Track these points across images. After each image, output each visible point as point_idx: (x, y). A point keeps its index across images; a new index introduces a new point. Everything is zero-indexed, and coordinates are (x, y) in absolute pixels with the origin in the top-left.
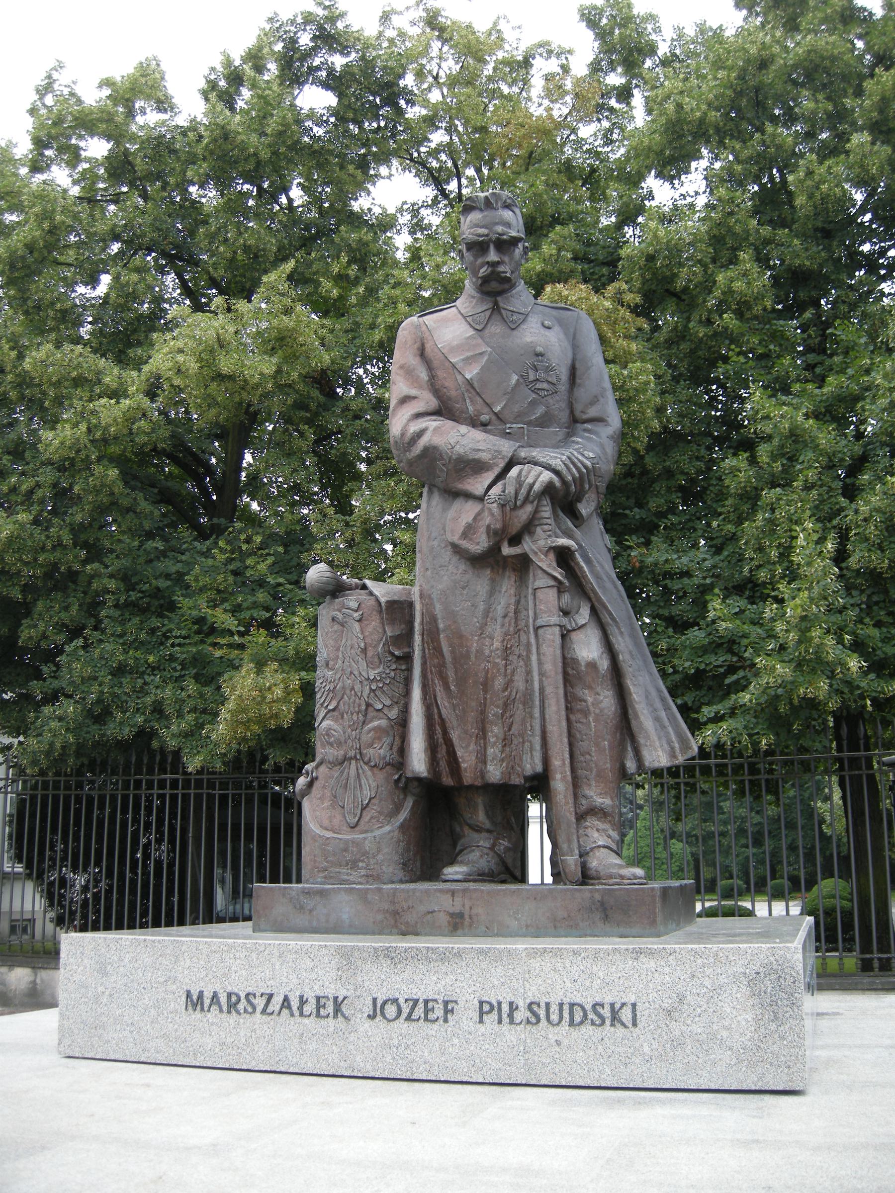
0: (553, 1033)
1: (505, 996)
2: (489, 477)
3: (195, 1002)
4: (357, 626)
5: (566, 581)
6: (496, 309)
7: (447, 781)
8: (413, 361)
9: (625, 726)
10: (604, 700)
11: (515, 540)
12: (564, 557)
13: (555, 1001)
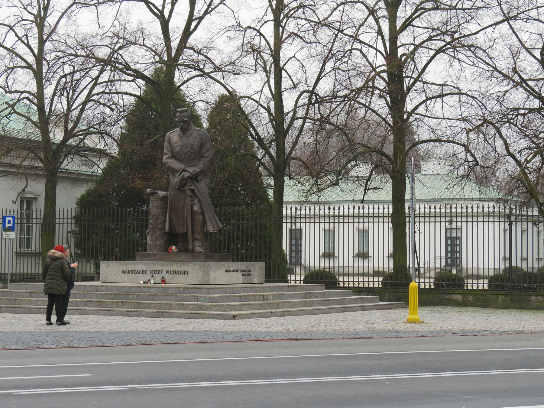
0: (177, 276)
1: (169, 270)
3: (123, 272)
6: (184, 133)
7: (174, 232)
8: (168, 145)
9: (204, 223)
10: (200, 218)
11: (183, 187)
12: (192, 191)
13: (177, 270)
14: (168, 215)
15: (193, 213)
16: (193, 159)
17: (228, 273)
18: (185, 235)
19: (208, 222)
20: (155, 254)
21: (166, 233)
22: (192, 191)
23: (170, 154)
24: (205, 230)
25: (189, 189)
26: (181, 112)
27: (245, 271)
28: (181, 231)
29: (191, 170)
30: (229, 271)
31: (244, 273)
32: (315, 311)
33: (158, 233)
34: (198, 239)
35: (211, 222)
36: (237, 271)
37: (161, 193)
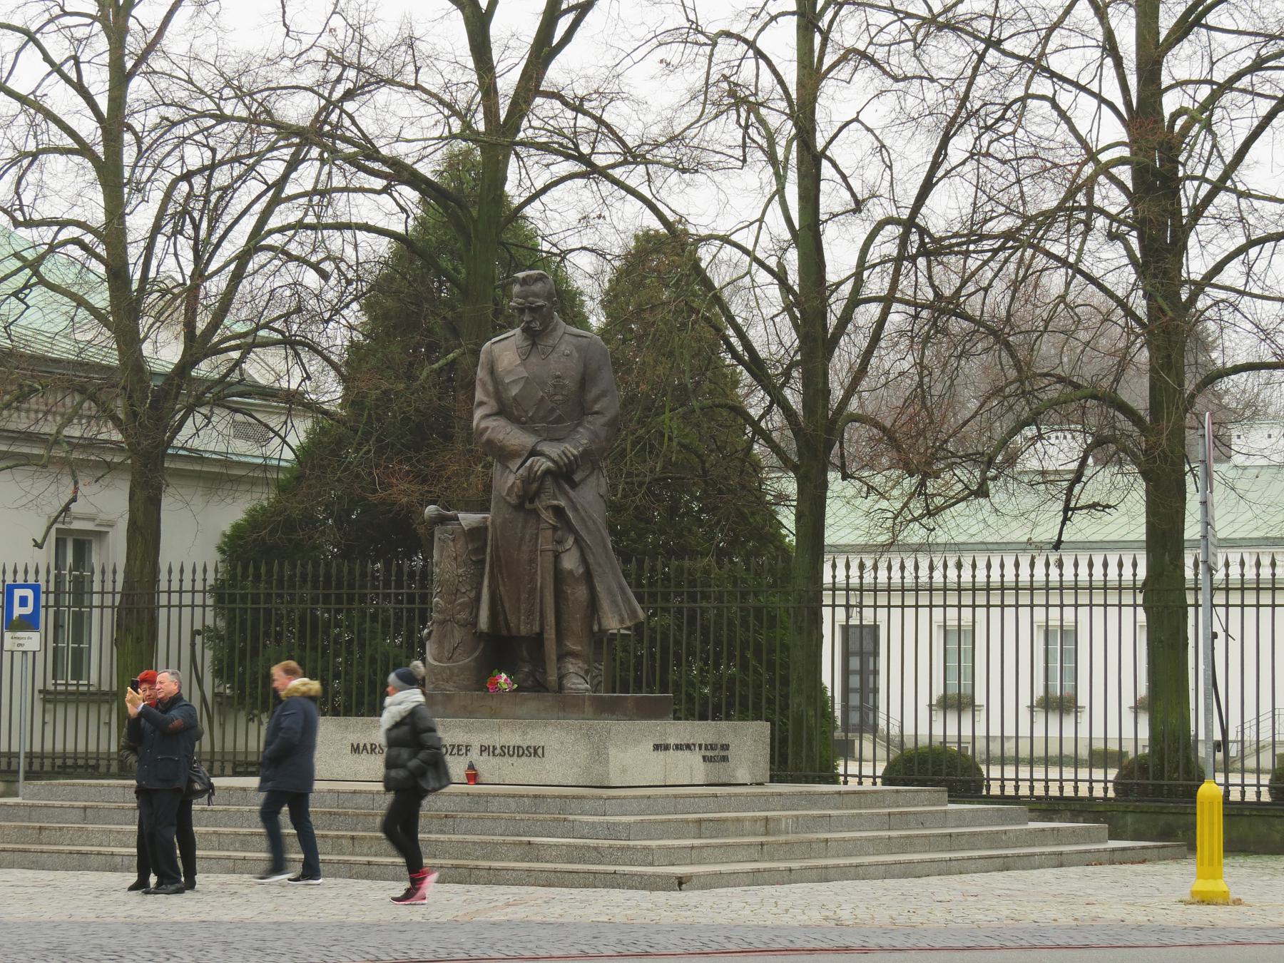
0: (511, 760)
2: (519, 461)
3: (356, 749)
4: (451, 544)
6: (534, 344)
7: (504, 632)
8: (487, 379)
9: (593, 606)
10: (581, 592)
11: (532, 501)
13: (512, 744)
14: (486, 582)
15: (559, 576)
16: (559, 420)
17: (661, 755)
18: (537, 641)
19: (605, 604)
20: (448, 698)
21: (480, 636)
22: (558, 511)
23: (492, 405)
24: (596, 628)
25: (547, 508)
26: (524, 282)
27: (712, 747)
28: (524, 630)
29: (553, 450)
30: (667, 747)
31: (709, 753)
32: (919, 867)
33: (456, 634)
34: (575, 655)
35: (614, 602)
36: (688, 747)
37: (468, 519)
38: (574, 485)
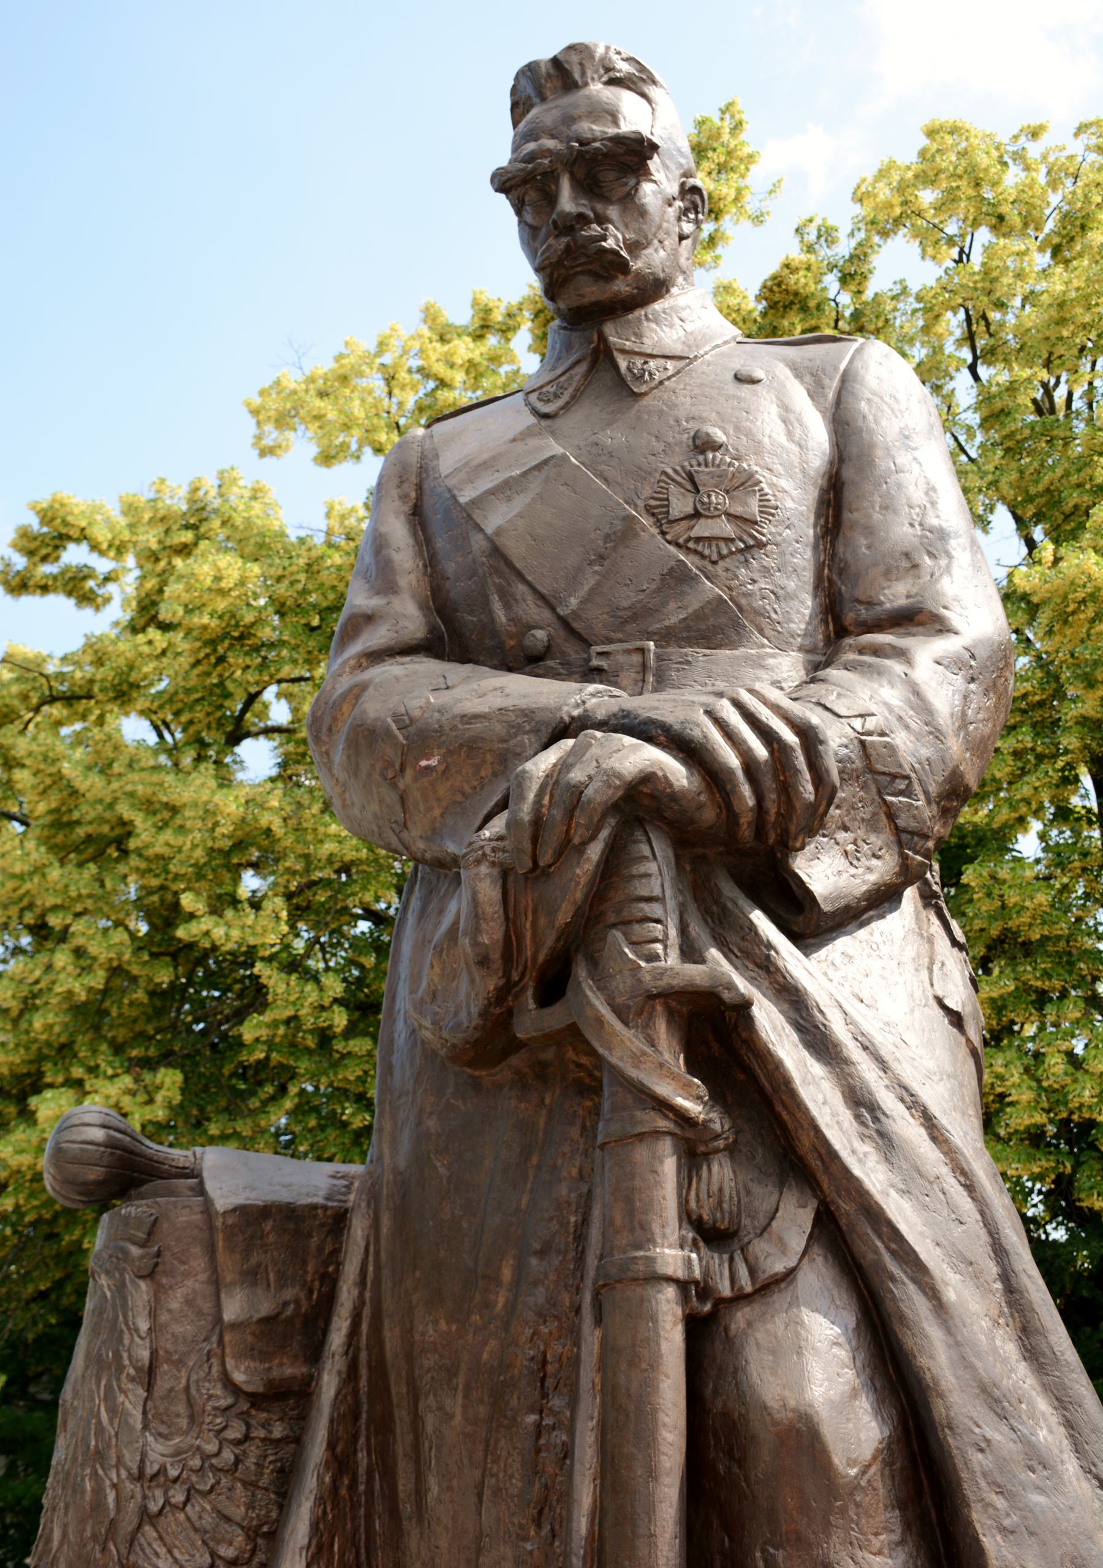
5: (718, 1122)
22: (716, 1035)
38: (810, 922)
